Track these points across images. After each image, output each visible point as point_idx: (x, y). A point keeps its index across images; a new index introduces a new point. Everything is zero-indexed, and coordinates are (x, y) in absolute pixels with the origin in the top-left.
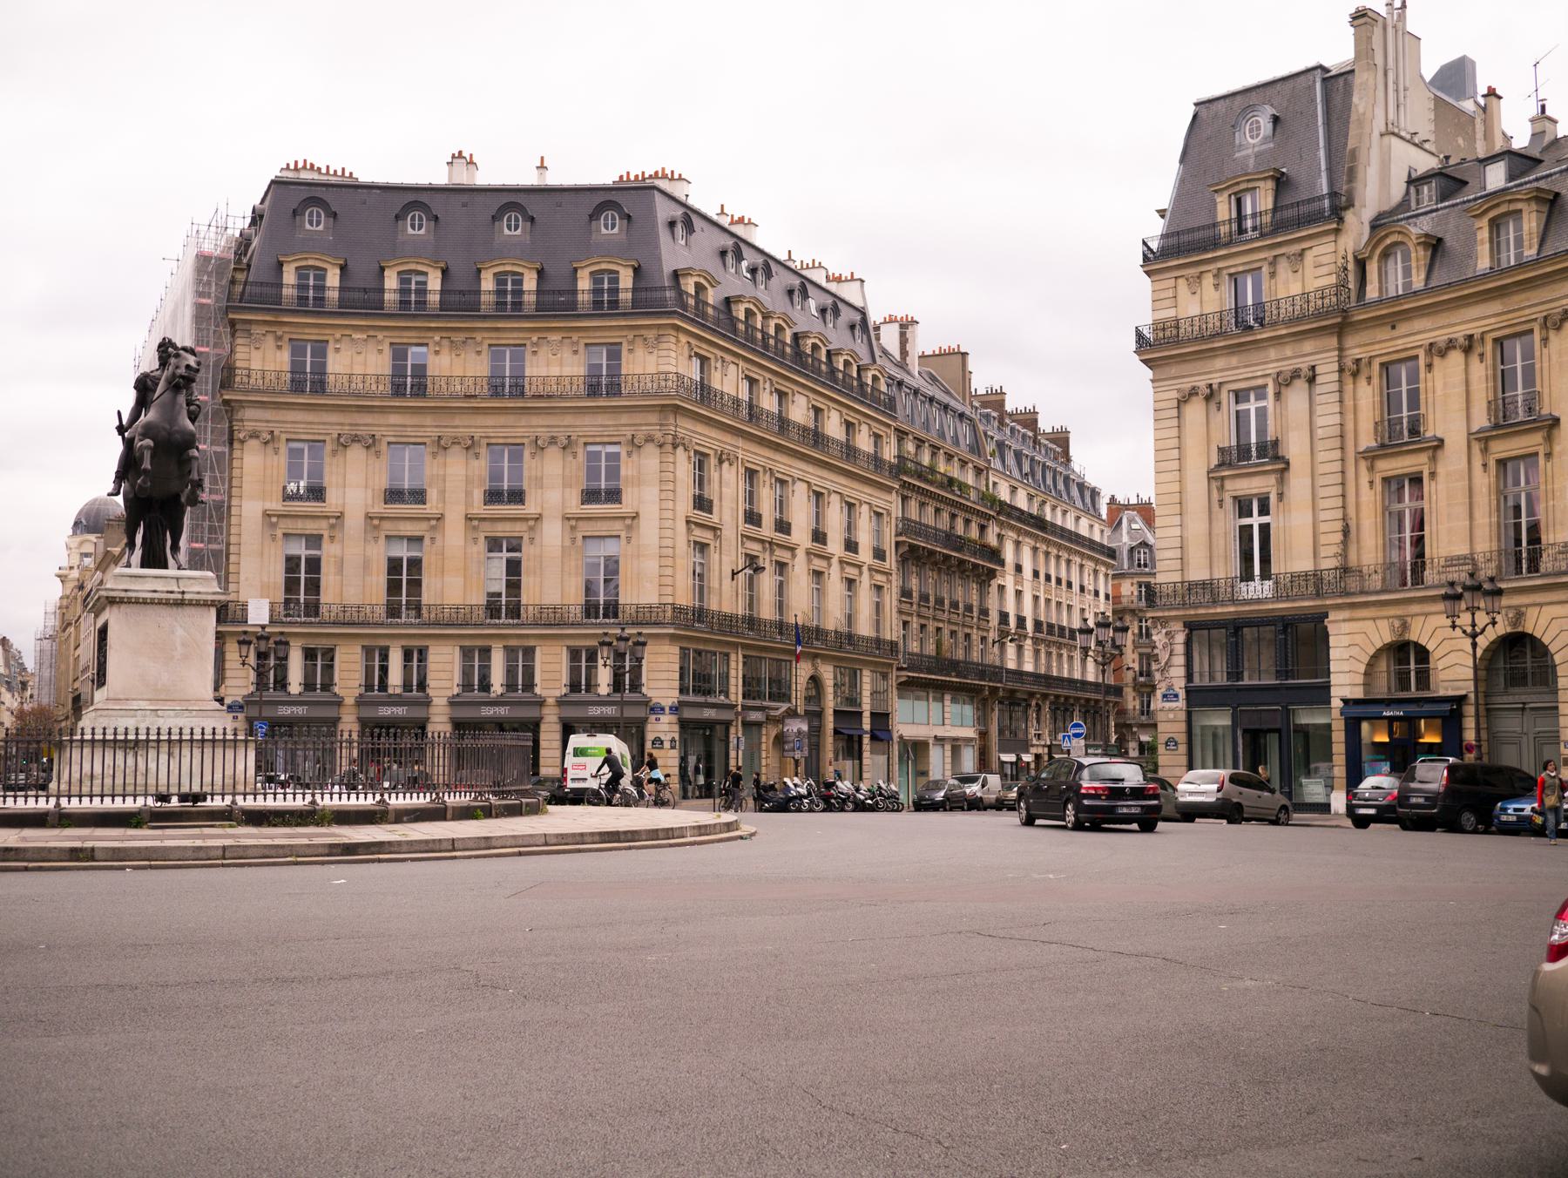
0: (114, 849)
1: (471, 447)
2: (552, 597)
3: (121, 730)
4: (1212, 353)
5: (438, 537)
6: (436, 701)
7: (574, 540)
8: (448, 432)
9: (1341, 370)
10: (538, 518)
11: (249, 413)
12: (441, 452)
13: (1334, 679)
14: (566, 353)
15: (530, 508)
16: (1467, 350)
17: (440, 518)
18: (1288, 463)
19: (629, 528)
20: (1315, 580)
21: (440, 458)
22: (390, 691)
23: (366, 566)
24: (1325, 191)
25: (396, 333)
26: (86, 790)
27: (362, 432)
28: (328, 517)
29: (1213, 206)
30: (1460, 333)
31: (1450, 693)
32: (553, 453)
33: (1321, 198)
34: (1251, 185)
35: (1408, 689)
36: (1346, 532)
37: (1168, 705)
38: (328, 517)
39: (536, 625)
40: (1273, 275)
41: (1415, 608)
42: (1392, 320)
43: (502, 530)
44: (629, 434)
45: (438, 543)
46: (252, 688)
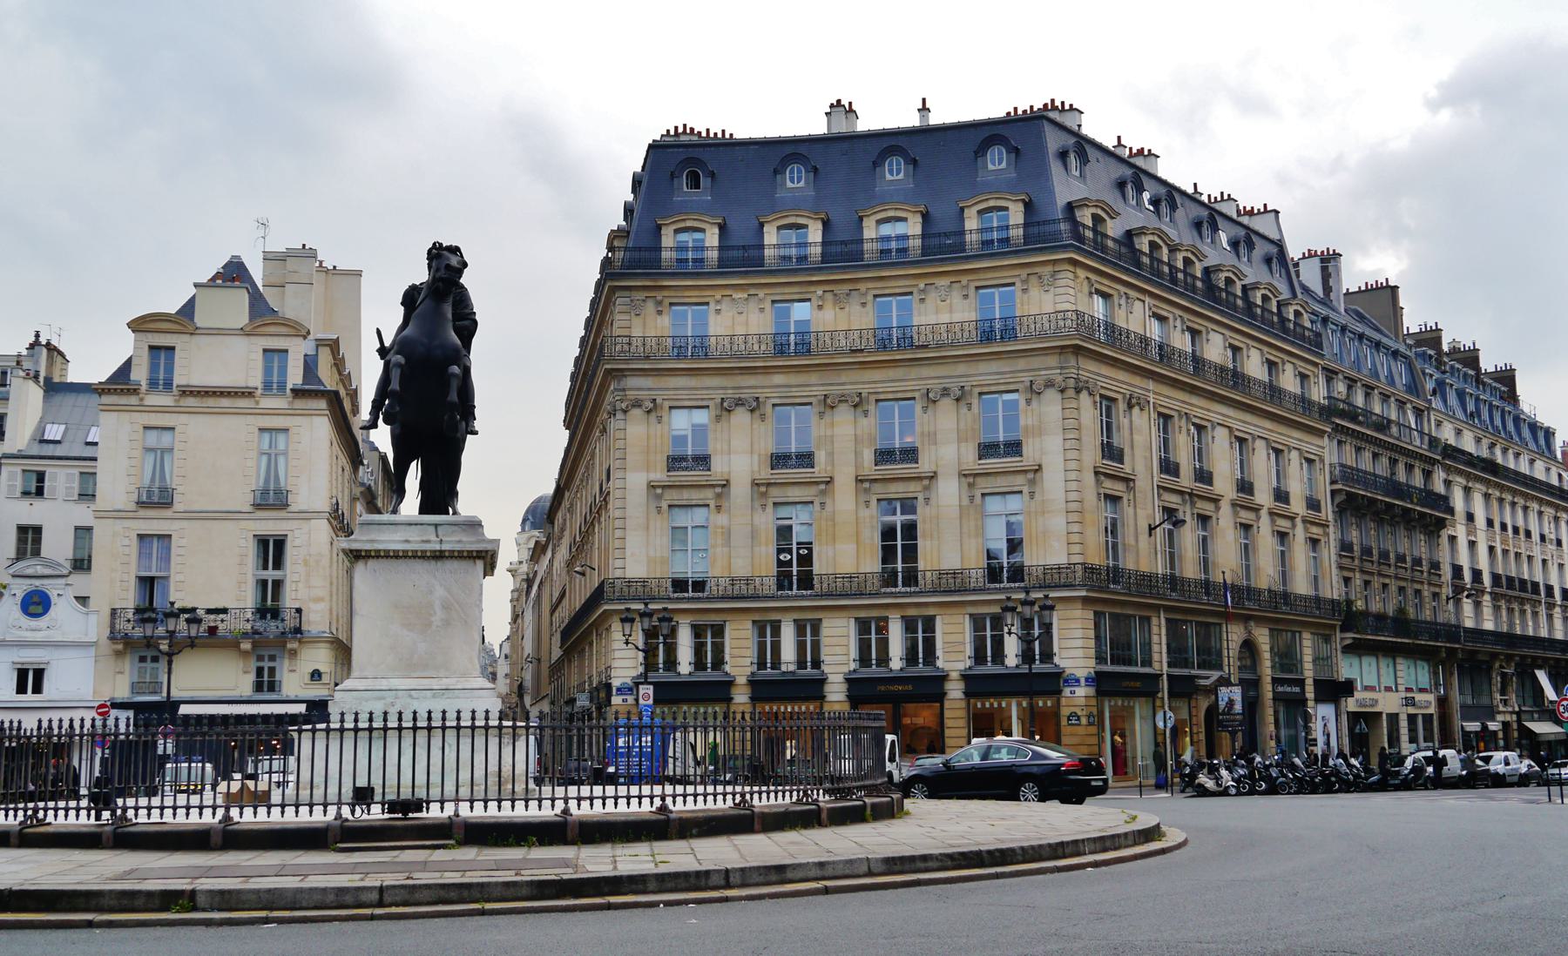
0: (222, 892)
1: (858, 404)
2: (951, 562)
5: (829, 502)
6: (831, 678)
7: (972, 498)
10: (933, 477)
11: (632, 382)
12: (828, 412)
14: (956, 297)
15: (925, 465)
17: (830, 482)
19: (1032, 482)
21: (827, 418)
22: (784, 668)
23: (754, 534)
25: (778, 290)
26: (318, 794)
27: (746, 394)
28: (713, 486)
32: (946, 404)
38: (713, 486)
39: (934, 592)
43: (897, 490)
45: (829, 507)
46: (641, 669)
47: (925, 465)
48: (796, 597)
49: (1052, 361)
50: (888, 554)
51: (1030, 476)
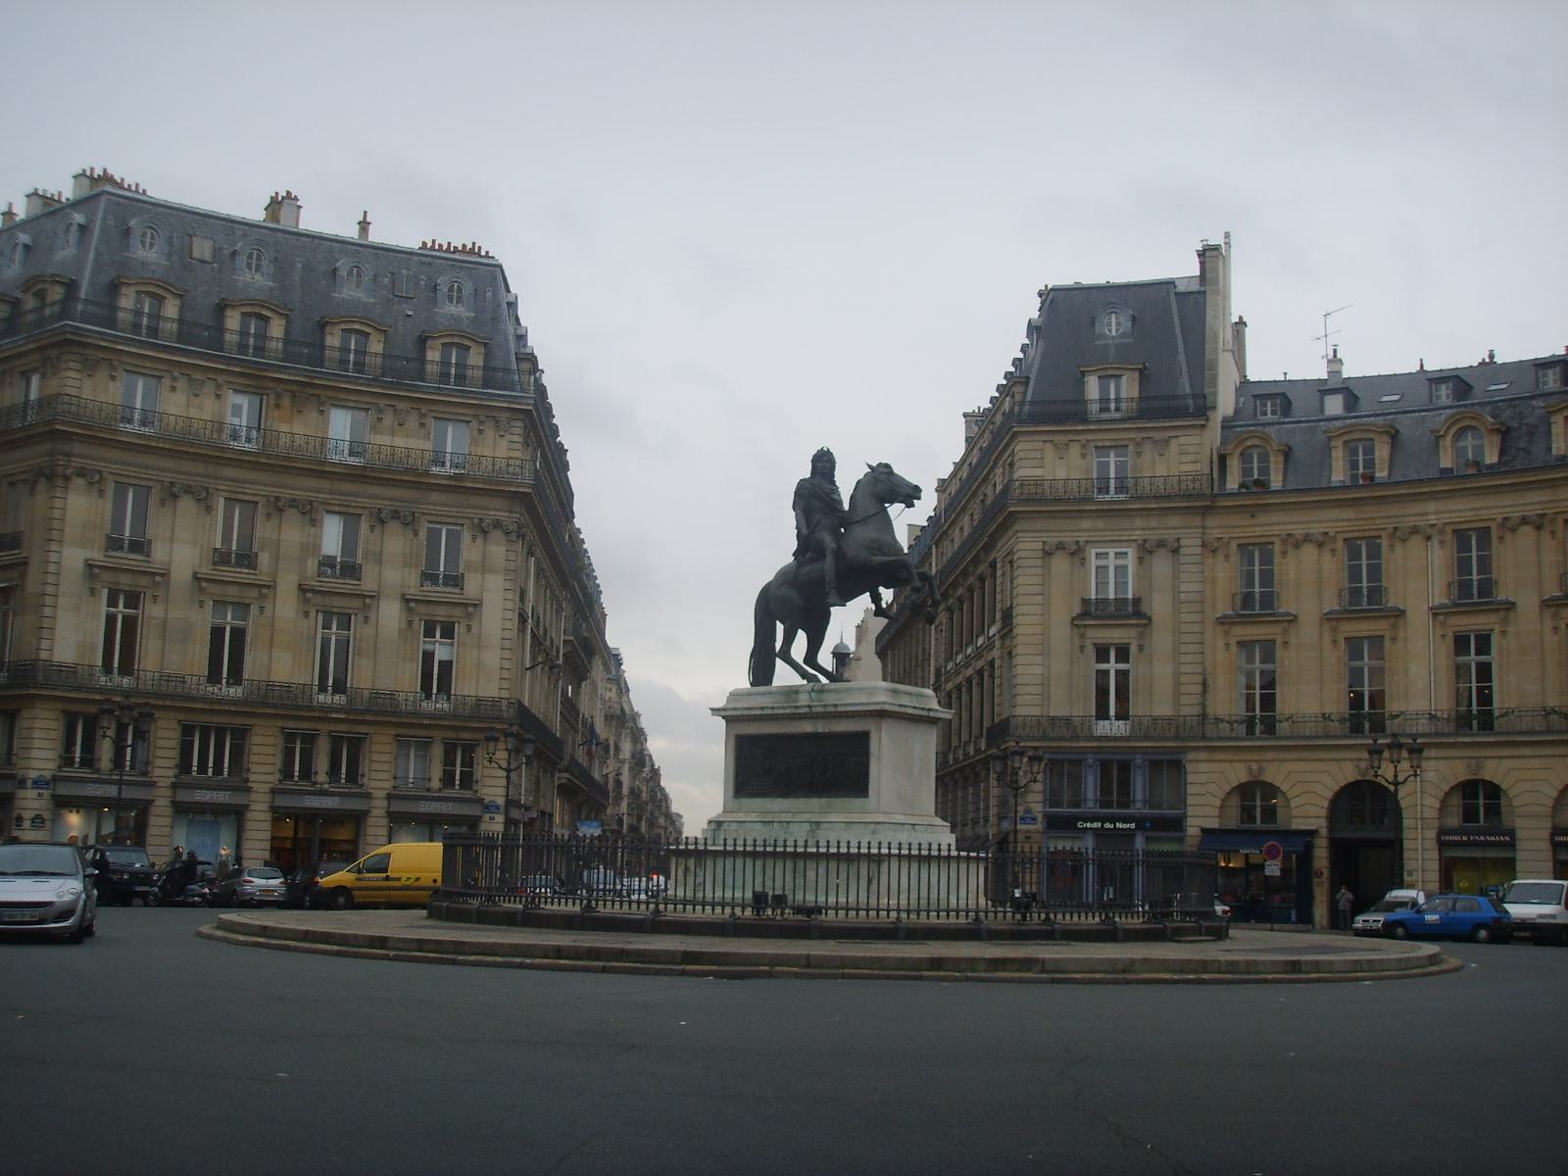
3: (925, 846)
4: (1081, 514)
8: (286, 493)
9: (1203, 545)
13: (1190, 811)
15: (368, 584)
16: (1320, 545)
17: (271, 587)
18: (1150, 619)
20: (1174, 726)
24: (1188, 391)
29: (1080, 384)
30: (1316, 529)
31: (1302, 827)
33: (1185, 396)
34: (1118, 373)
35: (1255, 823)
36: (1204, 684)
40: (1139, 454)
41: (1270, 755)
42: (1252, 511)
45: (268, 612)
47: (368, 584)
49: (498, 503)
51: (470, 609)
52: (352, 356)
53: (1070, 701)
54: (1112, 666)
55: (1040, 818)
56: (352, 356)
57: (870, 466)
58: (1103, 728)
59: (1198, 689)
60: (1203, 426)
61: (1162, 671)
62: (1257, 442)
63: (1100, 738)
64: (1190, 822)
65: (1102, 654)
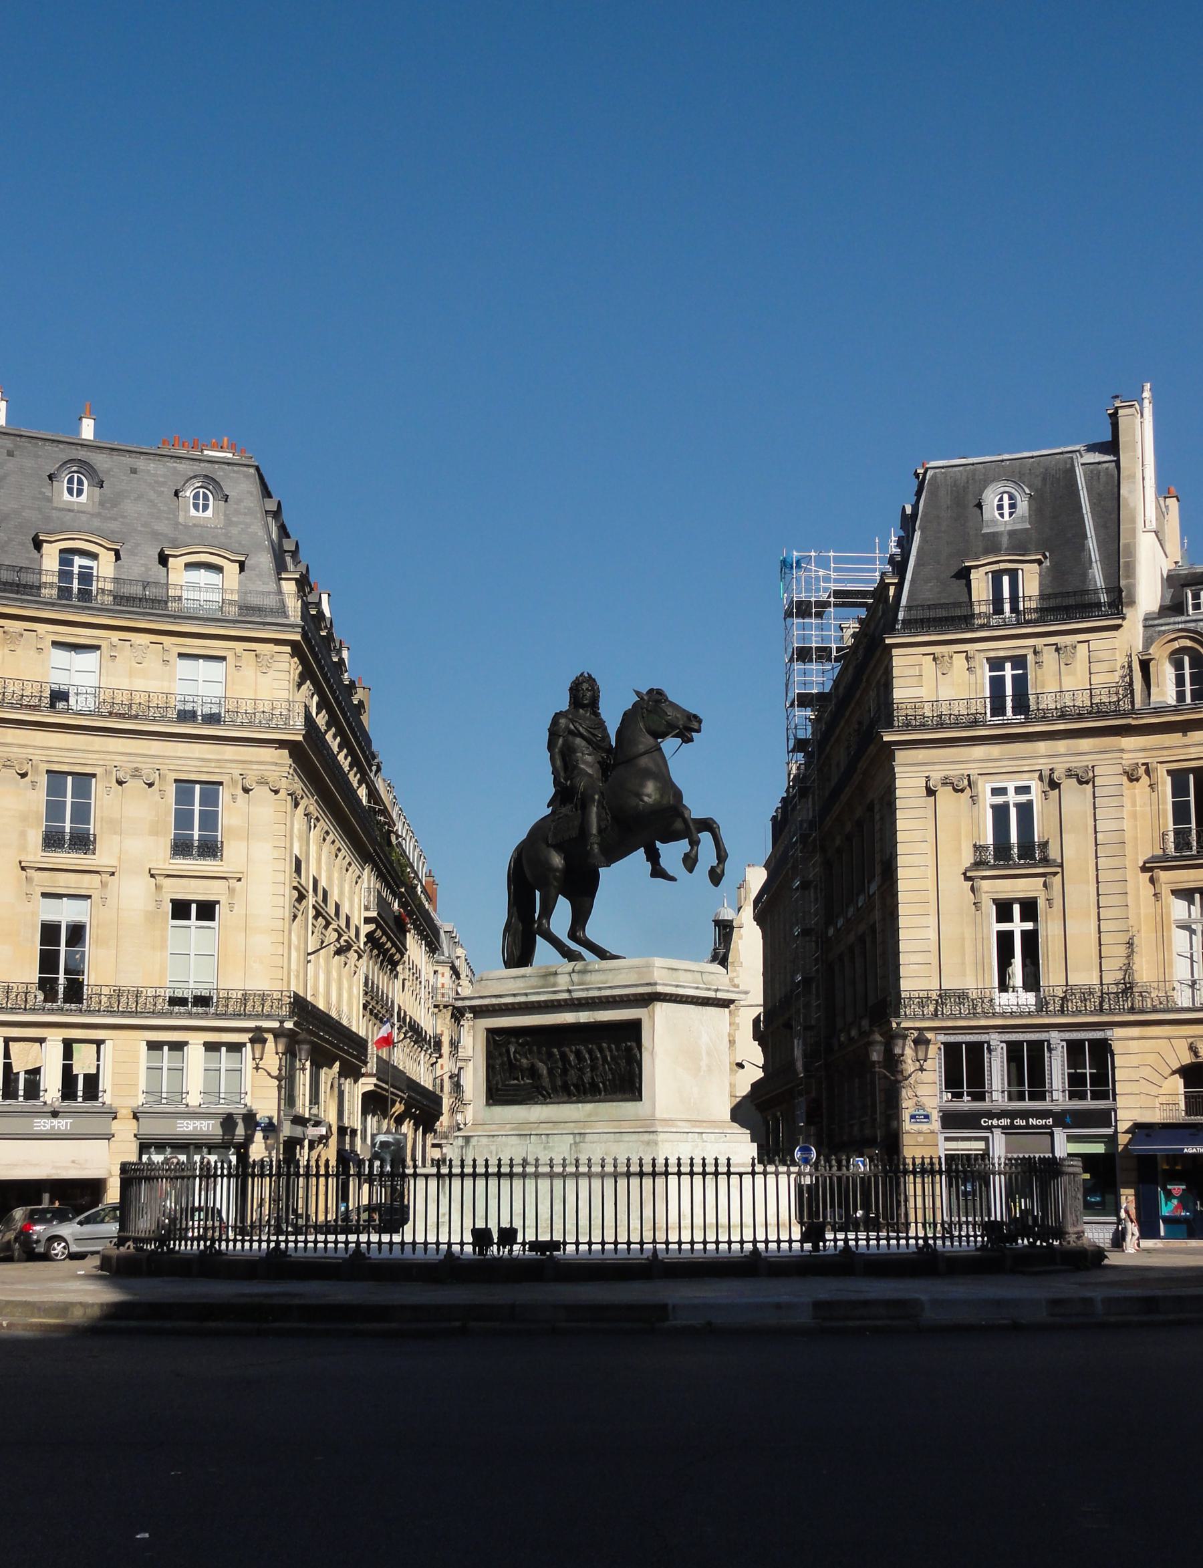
2: (130, 979)
13: (1121, 1101)
15: (102, 857)
37: (916, 1127)
39: (110, 1012)
44: (236, 772)
48: (61, 1011)
50: (48, 962)
52: (76, 581)
53: (971, 970)
54: (1017, 926)
55: (935, 1116)
56: (76, 581)
57: (638, 693)
58: (1004, 1000)
59: (1122, 950)
60: (1120, 626)
61: (1082, 929)
62: (1188, 643)
63: (1003, 1015)
64: (1121, 1114)
65: (1004, 911)
